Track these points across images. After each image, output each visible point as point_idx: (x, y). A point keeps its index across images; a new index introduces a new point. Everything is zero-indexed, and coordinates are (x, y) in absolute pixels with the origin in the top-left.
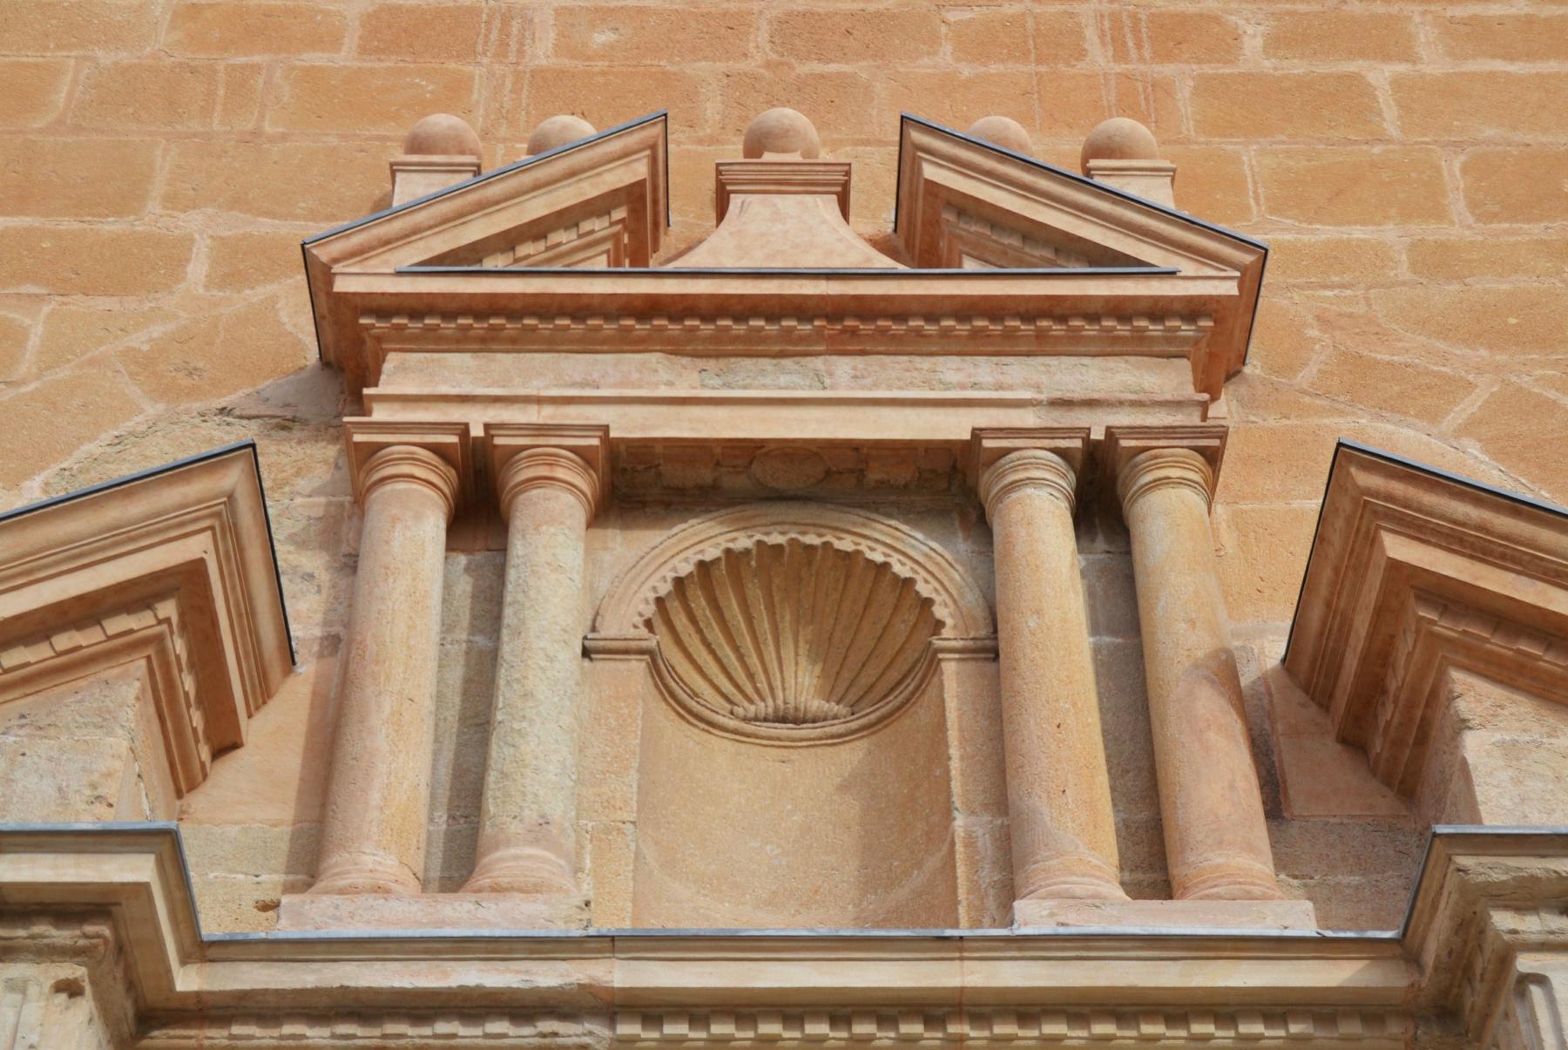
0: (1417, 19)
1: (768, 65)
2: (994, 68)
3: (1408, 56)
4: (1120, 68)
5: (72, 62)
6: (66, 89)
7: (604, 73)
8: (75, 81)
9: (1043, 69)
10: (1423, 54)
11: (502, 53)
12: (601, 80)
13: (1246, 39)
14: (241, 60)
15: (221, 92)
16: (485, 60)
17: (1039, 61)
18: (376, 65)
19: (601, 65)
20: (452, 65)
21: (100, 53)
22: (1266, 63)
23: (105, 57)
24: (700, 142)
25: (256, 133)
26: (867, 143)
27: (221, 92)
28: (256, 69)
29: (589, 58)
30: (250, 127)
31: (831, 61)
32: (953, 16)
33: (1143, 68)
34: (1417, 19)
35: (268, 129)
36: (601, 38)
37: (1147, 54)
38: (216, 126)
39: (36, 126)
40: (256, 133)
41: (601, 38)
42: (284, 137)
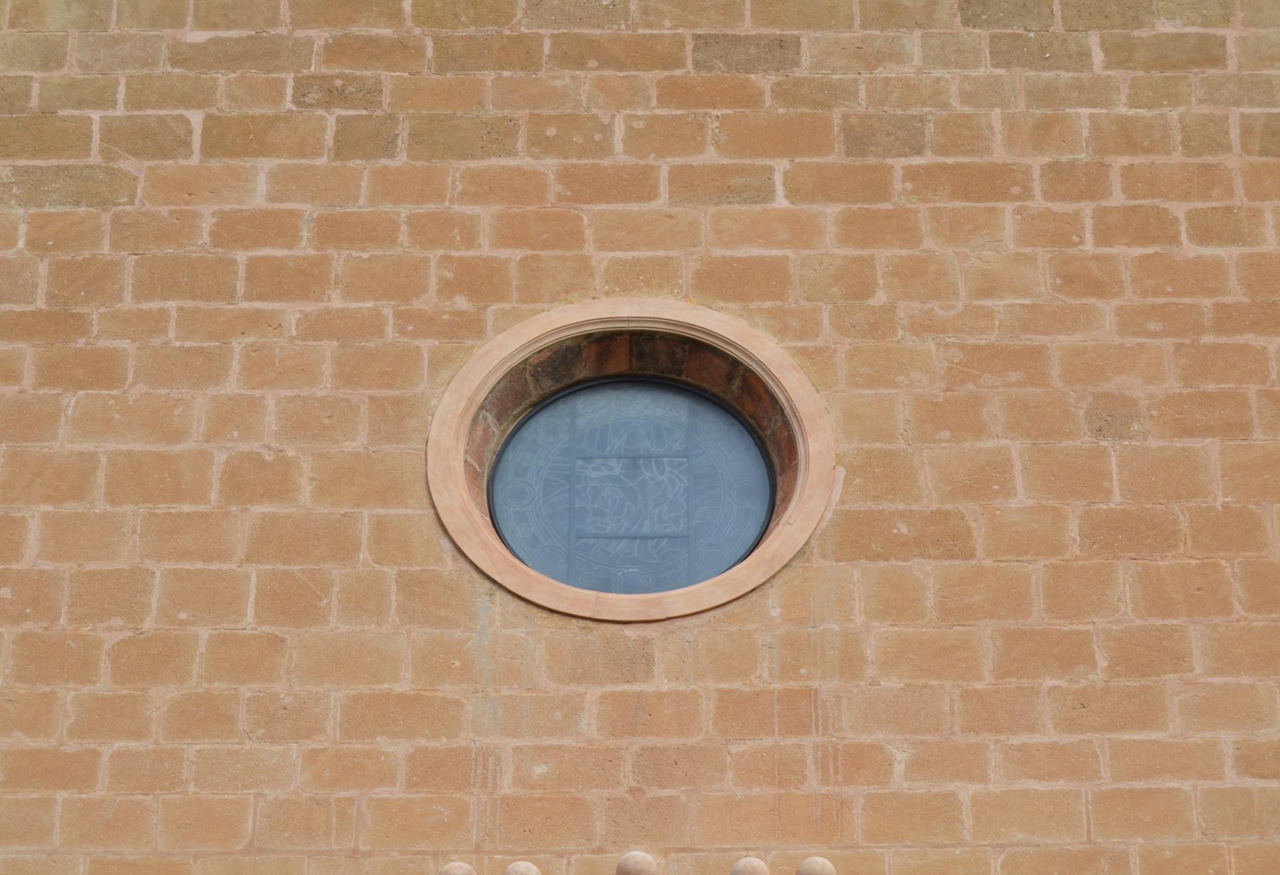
0: (992, 746)
1: (632, 791)
2: (756, 791)
3: (984, 779)
4: (824, 790)
5: (252, 798)
6: (251, 820)
7: (540, 799)
8: (255, 814)
9: (782, 791)
10: (992, 775)
11: (484, 786)
12: (539, 804)
13: (896, 765)
14: (342, 794)
15: (334, 819)
16: (476, 791)
17: (780, 786)
18: (416, 796)
19: (538, 793)
20: (458, 795)
21: (266, 791)
22: (905, 785)
23: (271, 794)
24: (593, 852)
25: (355, 851)
26: (682, 850)
27: (334, 819)
28: (350, 800)
29: (533, 788)
30: (352, 846)
31: (665, 787)
32: (736, 749)
33: (837, 789)
34: (992, 746)
35: (362, 848)
36: (540, 770)
37: (840, 779)
38: (334, 847)
39: (239, 848)
40: (355, 851)
41: (540, 770)
42: (370, 854)
